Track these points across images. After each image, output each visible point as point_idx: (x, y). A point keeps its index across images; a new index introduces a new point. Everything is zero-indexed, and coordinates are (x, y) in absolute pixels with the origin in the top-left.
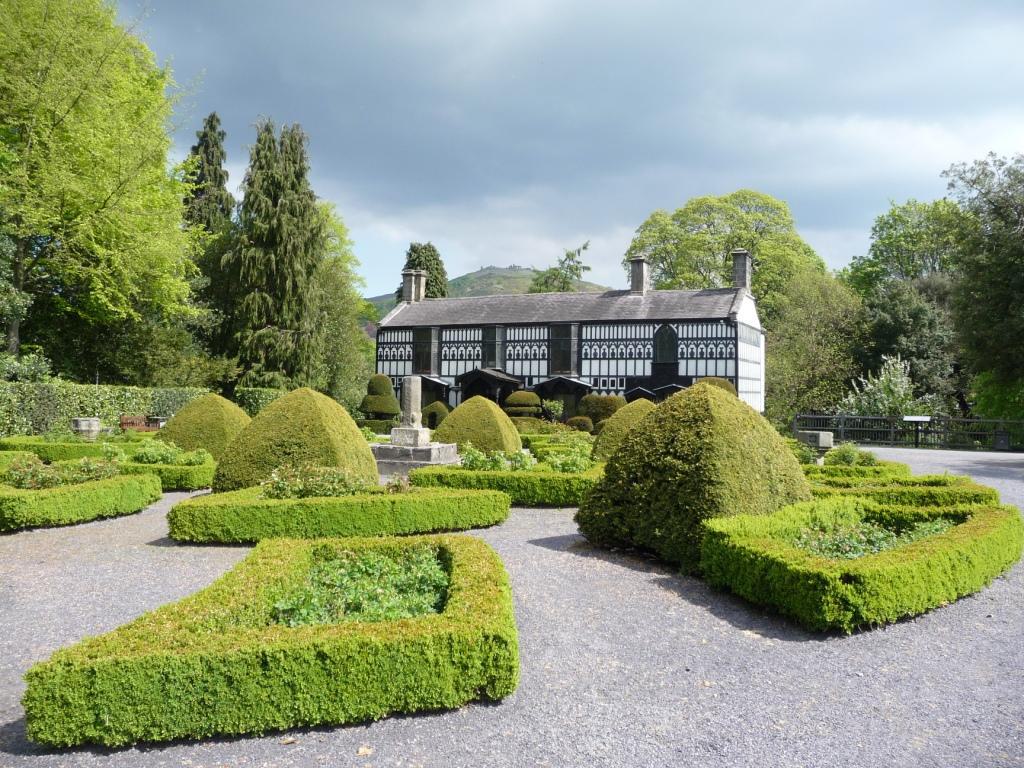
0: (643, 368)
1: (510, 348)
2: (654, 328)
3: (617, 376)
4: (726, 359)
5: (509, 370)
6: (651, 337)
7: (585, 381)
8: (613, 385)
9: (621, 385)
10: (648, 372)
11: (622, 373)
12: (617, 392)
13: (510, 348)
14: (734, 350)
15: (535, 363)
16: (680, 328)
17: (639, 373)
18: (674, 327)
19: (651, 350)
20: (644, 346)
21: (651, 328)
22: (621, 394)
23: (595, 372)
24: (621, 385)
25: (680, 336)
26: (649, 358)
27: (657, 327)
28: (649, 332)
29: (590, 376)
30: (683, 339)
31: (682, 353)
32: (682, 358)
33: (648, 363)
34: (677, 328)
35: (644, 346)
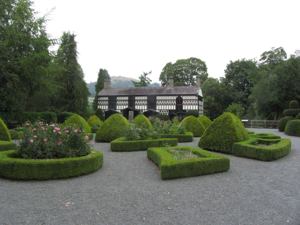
0: (173, 108)
1: (136, 102)
2: (176, 97)
3: (166, 110)
4: (188, 105)
5: (136, 108)
6: (175, 99)
7: (157, 111)
8: (165, 112)
9: (167, 112)
10: (175, 109)
11: (167, 109)
12: (166, 114)
13: (136, 102)
14: (197, 103)
15: (143, 106)
16: (183, 97)
17: (172, 109)
18: (181, 96)
19: (175, 103)
20: (174, 102)
21: (175, 97)
22: (167, 114)
23: (160, 109)
24: (167, 112)
25: (183, 99)
26: (175, 105)
27: (177, 96)
28: (175, 98)
29: (159, 110)
30: (184, 100)
31: (136, 104)
32: (184, 105)
33: (175, 106)
34: (182, 97)
35: (174, 102)
